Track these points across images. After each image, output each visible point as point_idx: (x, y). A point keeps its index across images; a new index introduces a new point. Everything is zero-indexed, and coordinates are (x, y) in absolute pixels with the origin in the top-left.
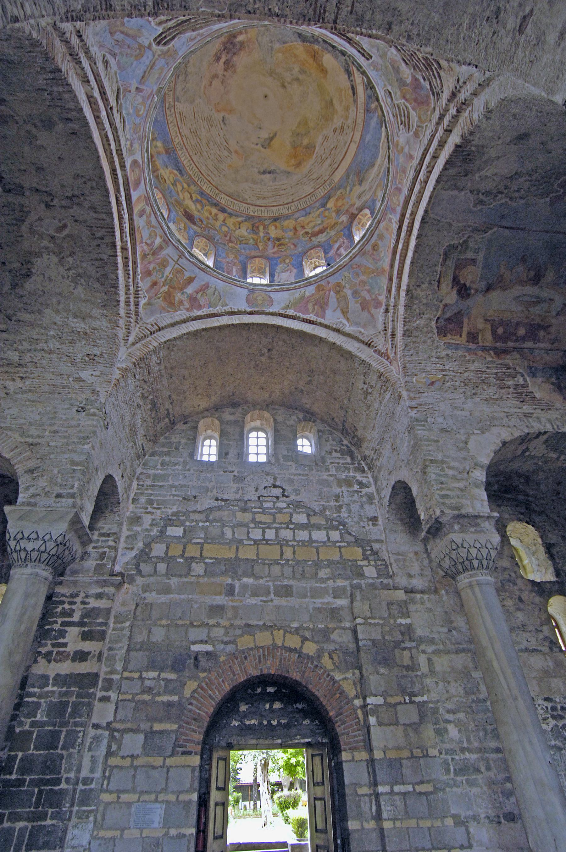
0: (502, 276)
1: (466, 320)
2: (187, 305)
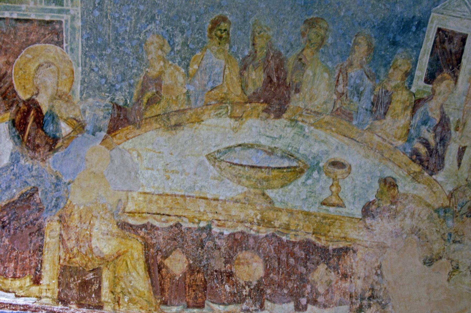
0: (158, 80)
1: (52, 228)
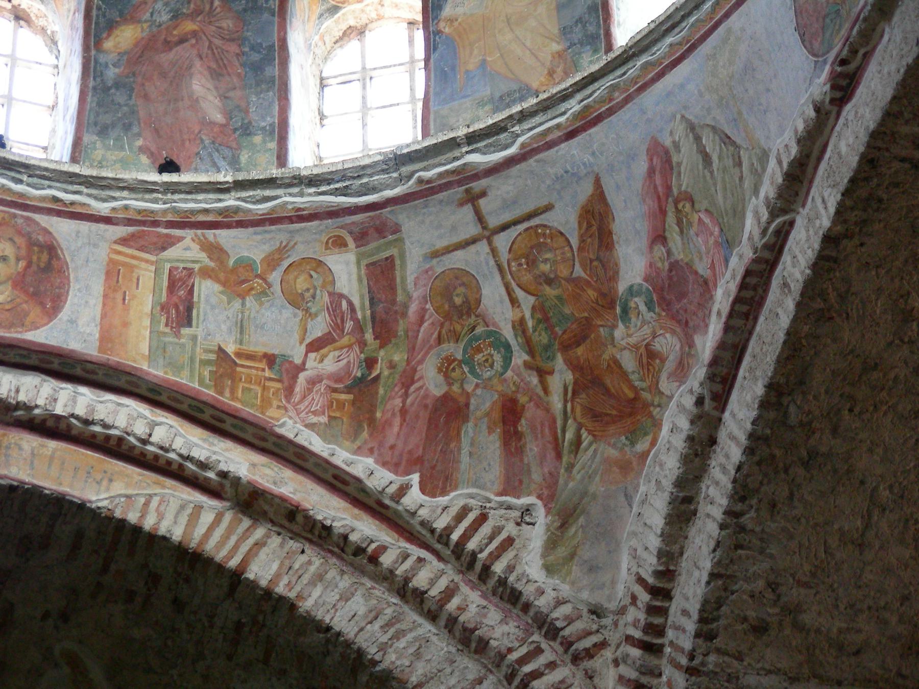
2: (668, 344)
